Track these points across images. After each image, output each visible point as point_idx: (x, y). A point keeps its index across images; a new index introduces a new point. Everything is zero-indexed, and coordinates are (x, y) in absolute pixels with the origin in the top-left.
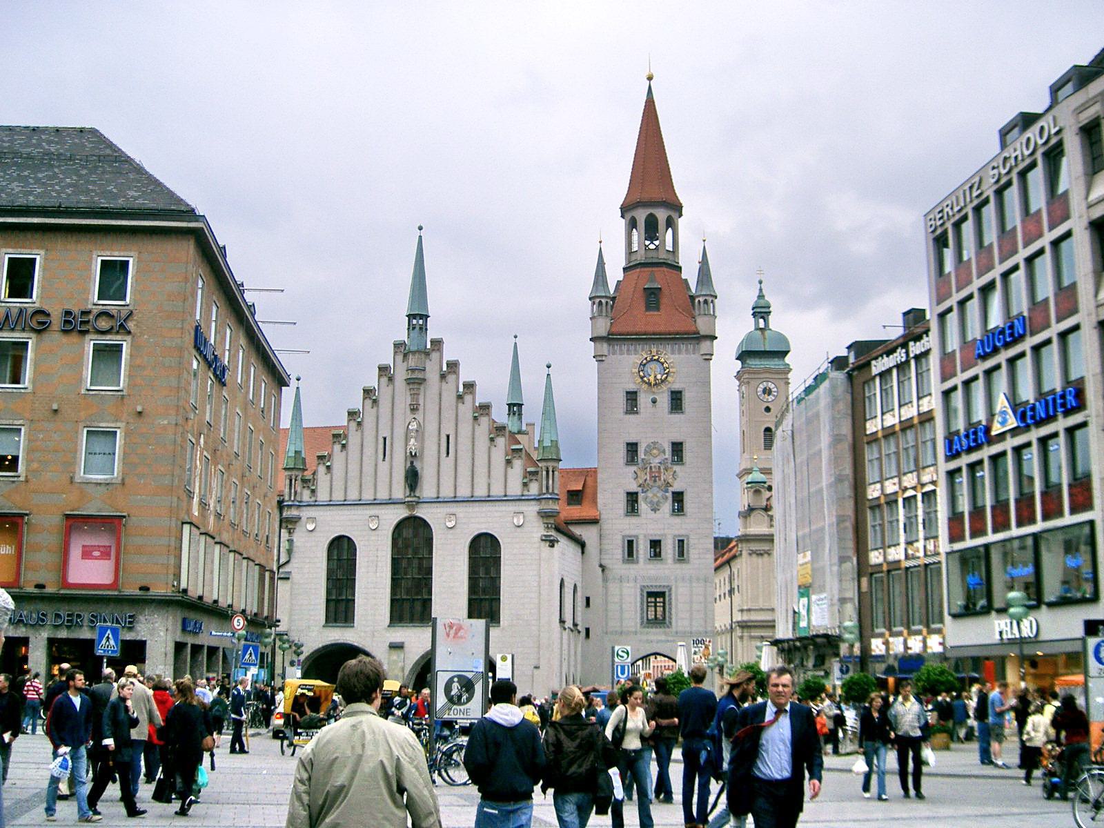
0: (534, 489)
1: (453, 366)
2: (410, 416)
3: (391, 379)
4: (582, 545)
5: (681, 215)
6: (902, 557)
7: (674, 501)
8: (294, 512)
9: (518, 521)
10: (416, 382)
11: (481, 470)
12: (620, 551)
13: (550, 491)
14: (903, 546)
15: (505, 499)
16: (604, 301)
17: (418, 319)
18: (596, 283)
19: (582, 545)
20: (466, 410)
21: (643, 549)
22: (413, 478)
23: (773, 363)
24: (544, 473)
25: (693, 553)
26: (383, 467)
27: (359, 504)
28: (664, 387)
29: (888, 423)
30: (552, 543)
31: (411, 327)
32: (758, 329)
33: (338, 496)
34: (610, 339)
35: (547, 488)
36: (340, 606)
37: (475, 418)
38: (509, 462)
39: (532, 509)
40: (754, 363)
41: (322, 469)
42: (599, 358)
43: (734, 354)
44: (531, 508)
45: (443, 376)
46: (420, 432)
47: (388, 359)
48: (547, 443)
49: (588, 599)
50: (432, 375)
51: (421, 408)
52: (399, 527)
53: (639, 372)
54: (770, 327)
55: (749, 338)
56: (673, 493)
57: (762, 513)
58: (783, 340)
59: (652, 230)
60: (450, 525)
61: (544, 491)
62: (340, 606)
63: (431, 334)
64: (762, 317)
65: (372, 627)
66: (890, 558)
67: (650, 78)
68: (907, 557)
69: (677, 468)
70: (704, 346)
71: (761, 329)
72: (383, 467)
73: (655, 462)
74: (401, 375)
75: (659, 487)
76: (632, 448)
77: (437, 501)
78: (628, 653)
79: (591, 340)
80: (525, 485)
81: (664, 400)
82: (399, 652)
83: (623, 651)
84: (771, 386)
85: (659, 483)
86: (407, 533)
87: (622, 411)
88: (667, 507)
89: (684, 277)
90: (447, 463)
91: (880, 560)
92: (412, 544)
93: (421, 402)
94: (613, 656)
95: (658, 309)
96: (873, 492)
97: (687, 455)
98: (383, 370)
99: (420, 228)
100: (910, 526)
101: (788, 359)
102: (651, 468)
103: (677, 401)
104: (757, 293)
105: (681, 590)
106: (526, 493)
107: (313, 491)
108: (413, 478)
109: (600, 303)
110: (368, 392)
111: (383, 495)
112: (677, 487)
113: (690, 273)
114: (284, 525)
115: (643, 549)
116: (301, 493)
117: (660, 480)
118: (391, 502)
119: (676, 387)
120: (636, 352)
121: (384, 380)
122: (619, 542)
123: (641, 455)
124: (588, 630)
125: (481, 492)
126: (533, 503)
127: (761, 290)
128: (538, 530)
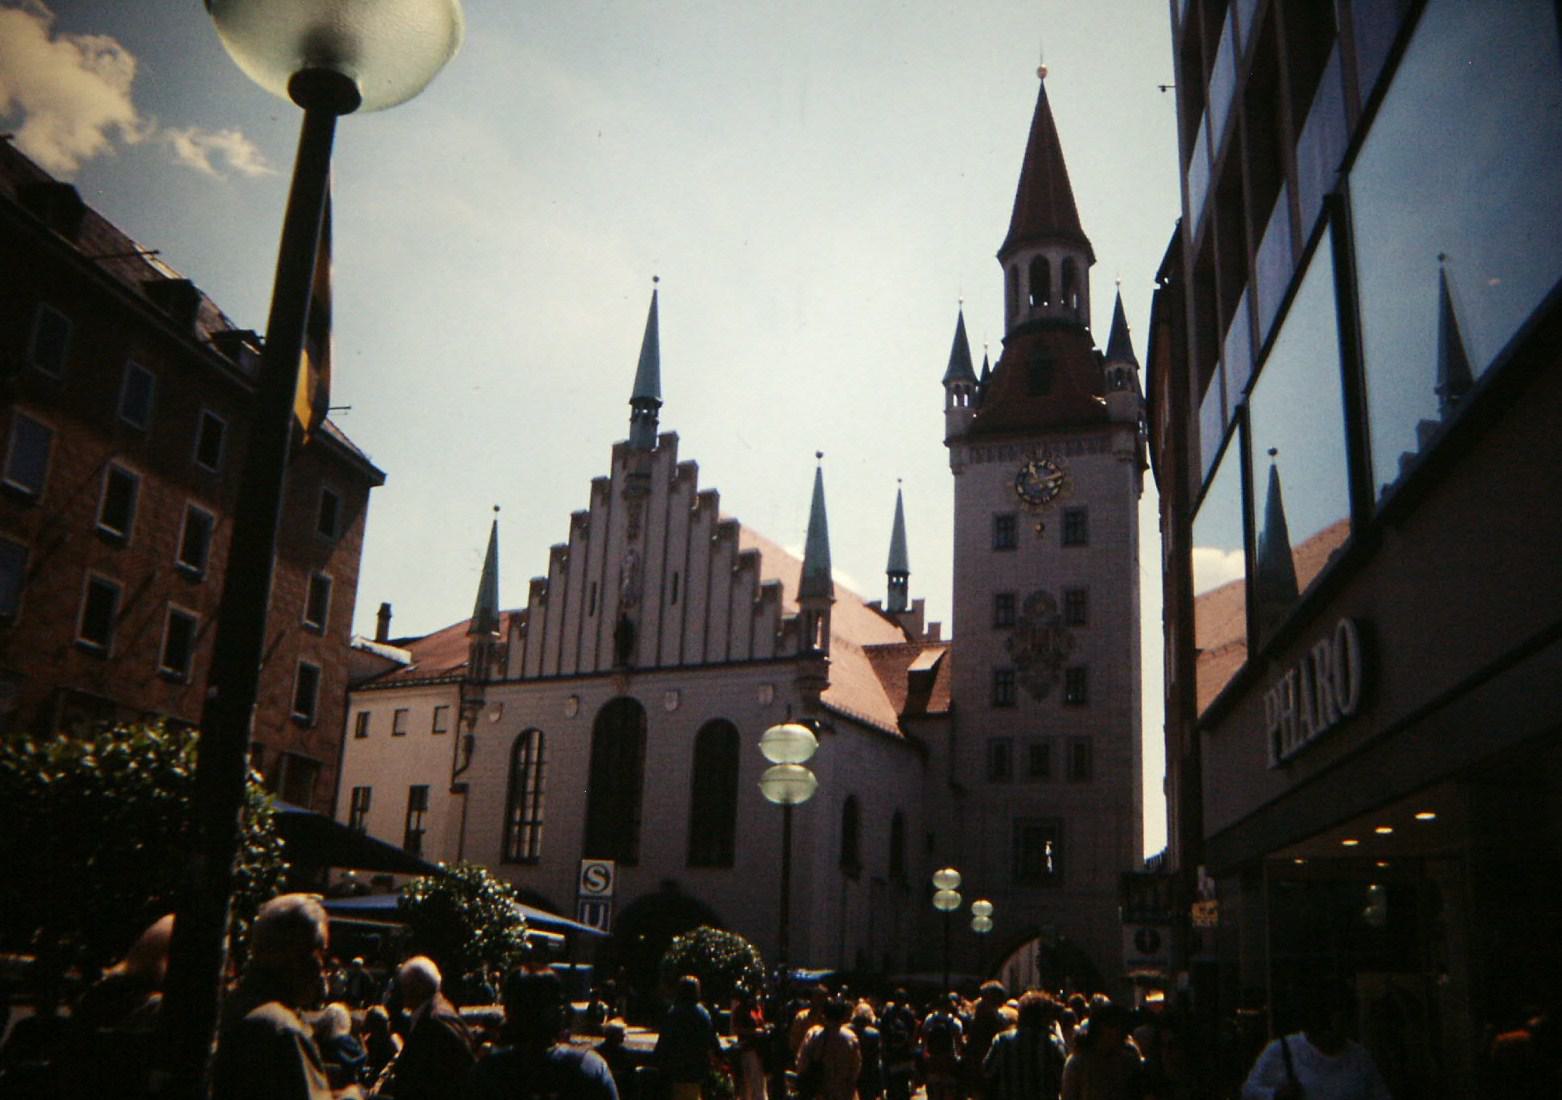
5: (1091, 260)
11: (718, 619)
20: (701, 534)
22: (626, 635)
26: (591, 623)
27: (559, 677)
34: (971, 439)
41: (515, 633)
42: (957, 467)
45: (673, 488)
47: (605, 470)
50: (659, 487)
51: (641, 537)
53: (1016, 487)
63: (662, 428)
67: (1042, 73)
69: (1074, 631)
74: (619, 487)
76: (1005, 601)
78: (606, 876)
80: (779, 643)
81: (1055, 525)
83: (597, 872)
88: (1057, 693)
89: (1094, 349)
90: (673, 613)
93: (643, 522)
94: (578, 884)
98: (599, 485)
99: (656, 279)
103: (1075, 527)
106: (781, 654)
107: (504, 669)
108: (626, 635)
111: (587, 666)
112: (1075, 658)
113: (1101, 339)
114: (467, 714)
116: (488, 669)
118: (597, 674)
123: (1021, 613)
125: (717, 654)
126: (792, 667)
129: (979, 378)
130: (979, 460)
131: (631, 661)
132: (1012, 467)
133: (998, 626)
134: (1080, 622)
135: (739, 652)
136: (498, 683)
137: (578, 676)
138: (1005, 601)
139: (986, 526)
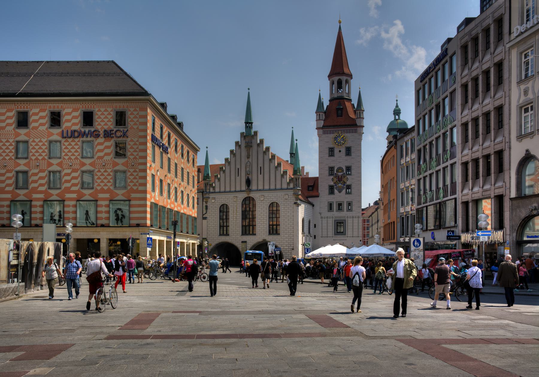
0: (292, 186)
1: (262, 141)
2: (247, 160)
3: (240, 146)
4: (313, 206)
6: (410, 210)
7: (347, 189)
8: (207, 196)
10: (249, 146)
12: (327, 207)
14: (410, 206)
16: (321, 114)
17: (249, 124)
19: (313, 206)
21: (335, 207)
22: (248, 182)
25: (354, 208)
27: (230, 192)
28: (344, 146)
29: (407, 161)
30: (298, 205)
31: (246, 127)
32: (396, 120)
33: (222, 189)
36: (224, 228)
37: (270, 160)
39: (291, 193)
41: (217, 180)
42: (319, 135)
43: (386, 130)
46: (251, 165)
49: (315, 225)
51: (251, 157)
52: (245, 200)
55: (392, 123)
59: (340, 85)
60: (262, 199)
62: (224, 228)
65: (235, 237)
66: (406, 210)
68: (411, 210)
69: (348, 177)
70: (358, 129)
71: (397, 120)
72: (238, 178)
73: (340, 174)
74: (243, 146)
76: (331, 169)
77: (258, 190)
80: (288, 184)
82: (245, 244)
85: (341, 182)
87: (327, 155)
90: (260, 177)
91: (403, 211)
92: (248, 206)
95: (341, 116)
96: (402, 186)
97: (353, 171)
98: (237, 143)
100: (412, 199)
104: (395, 105)
105: (349, 221)
106: (289, 187)
107: (214, 188)
108: (248, 182)
110: (232, 152)
111: (238, 189)
112: (348, 183)
114: (204, 200)
115: (335, 207)
118: (241, 191)
119: (348, 145)
120: (333, 133)
121: (238, 147)
122: (327, 204)
124: (315, 236)
127: (397, 104)
128: (293, 200)
131: (250, 188)
132: (332, 136)
135: (278, 187)
136: (212, 193)
137: (235, 191)
139: (327, 151)
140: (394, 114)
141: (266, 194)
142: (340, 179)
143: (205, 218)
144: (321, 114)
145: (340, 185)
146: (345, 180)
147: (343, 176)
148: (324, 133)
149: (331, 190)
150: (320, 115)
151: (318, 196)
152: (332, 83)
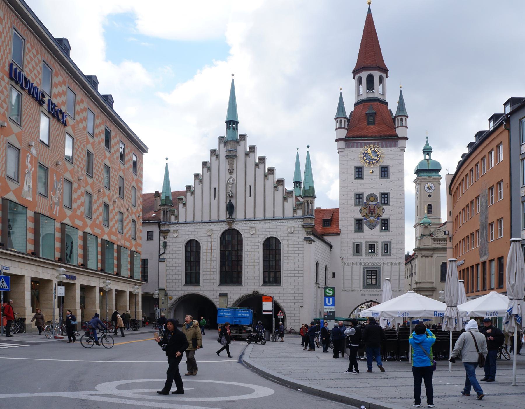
0: (300, 213)
9: (291, 230)
13: (310, 213)
15: (284, 219)
18: (339, 111)
23: (434, 175)
24: (306, 204)
32: (425, 159)
35: (308, 212)
38: (285, 199)
40: (423, 174)
44: (299, 223)
48: (307, 188)
54: (432, 158)
55: (421, 163)
56: (382, 220)
57: (429, 237)
58: (438, 164)
61: (306, 213)
64: (428, 154)
69: (384, 207)
73: (372, 203)
75: (374, 217)
76: (359, 196)
79: (336, 141)
80: (295, 211)
84: (432, 185)
85: (374, 215)
86: (228, 237)
87: (353, 177)
101: (440, 173)
102: (370, 207)
106: (295, 216)
109: (341, 121)
117: (375, 213)
127: (427, 141)
129: (348, 117)
130: (349, 148)
132: (361, 150)
133: (356, 205)
134: (387, 204)
135: (279, 215)
138: (359, 196)
140: (424, 153)
141: (258, 225)
142: (372, 211)
143: (162, 260)
144: (343, 120)
145: (372, 218)
146: (379, 211)
147: (377, 206)
148: (348, 147)
149: (359, 225)
150: (341, 121)
151: (338, 234)
152: (360, 81)
